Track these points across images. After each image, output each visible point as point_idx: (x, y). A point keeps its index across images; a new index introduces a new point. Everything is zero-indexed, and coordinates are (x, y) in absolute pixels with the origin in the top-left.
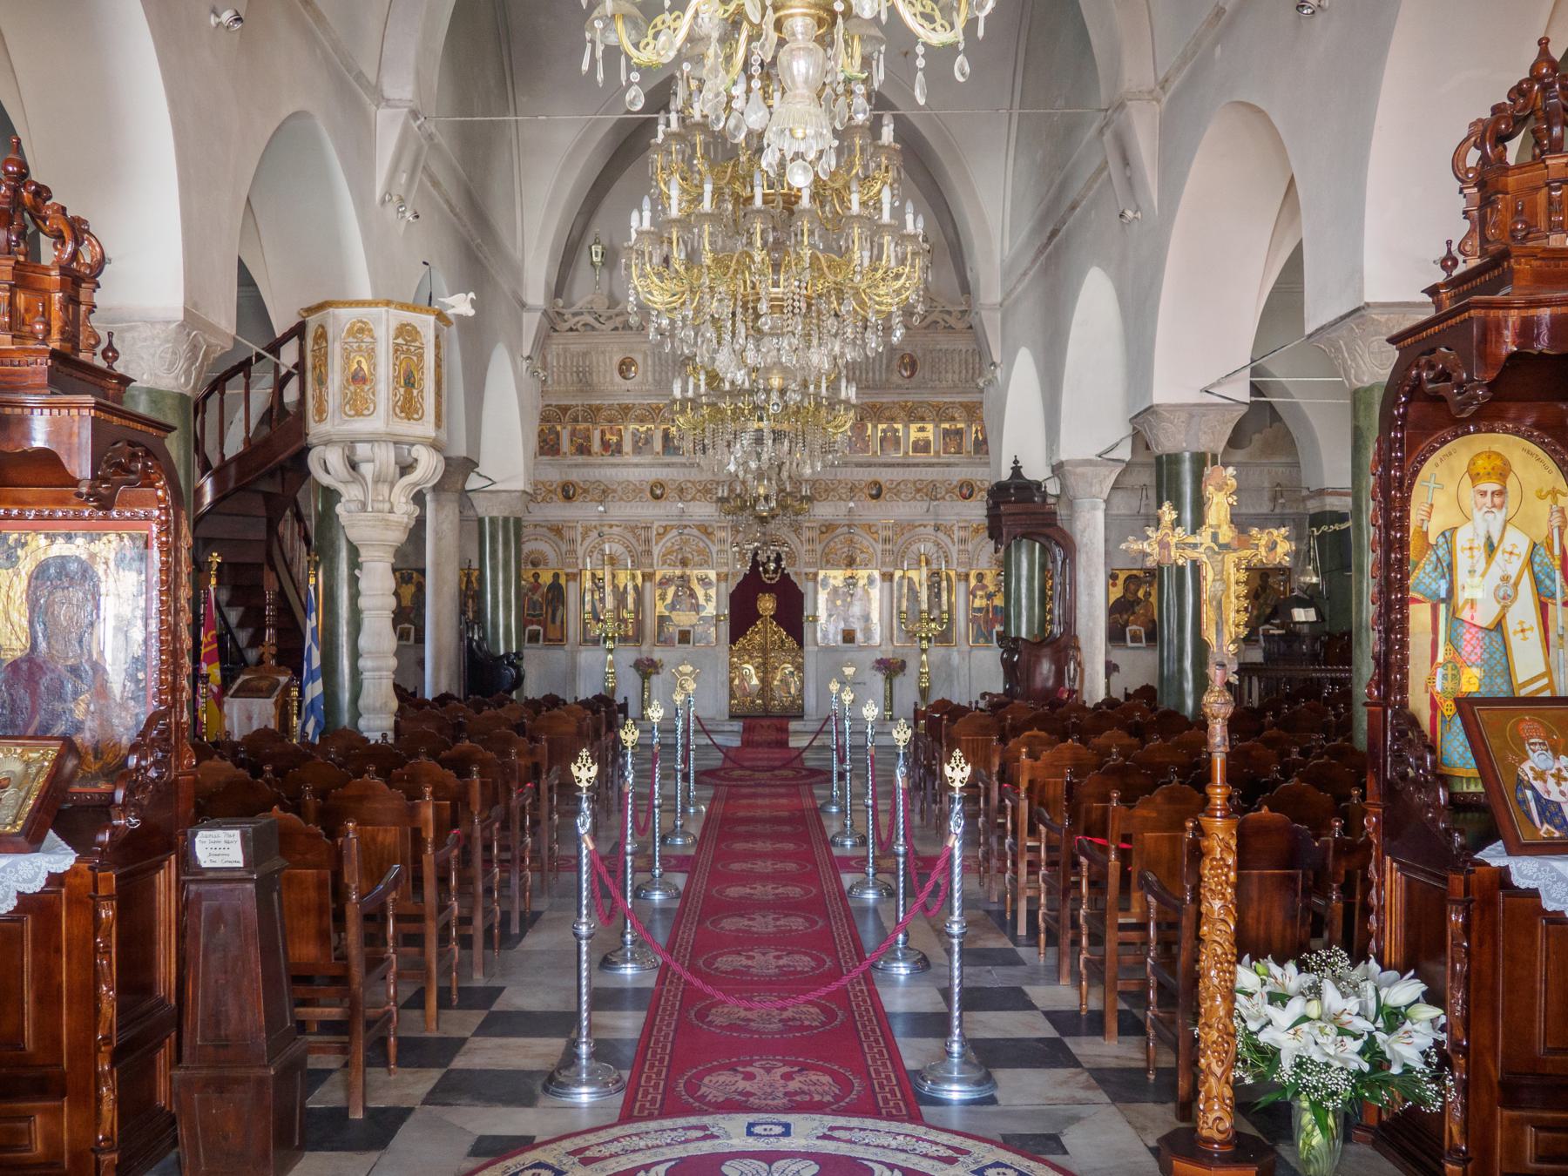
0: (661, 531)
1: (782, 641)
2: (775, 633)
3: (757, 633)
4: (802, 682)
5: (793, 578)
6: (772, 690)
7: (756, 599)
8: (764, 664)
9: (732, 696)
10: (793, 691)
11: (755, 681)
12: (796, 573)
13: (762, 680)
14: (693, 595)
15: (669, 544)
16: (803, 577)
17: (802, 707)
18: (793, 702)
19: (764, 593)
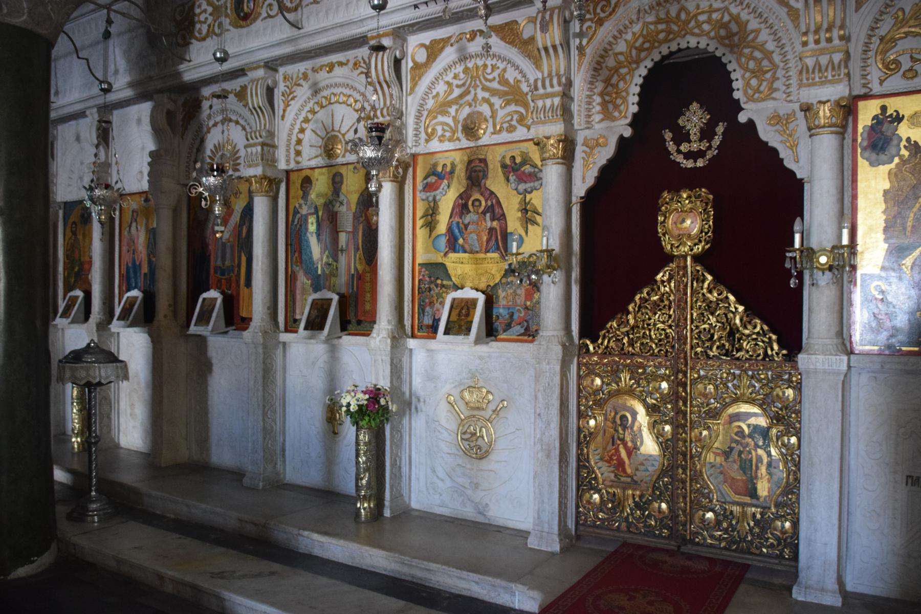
0: (422, 57)
1: (733, 332)
2: (711, 308)
3: (656, 307)
4: (793, 459)
5: (767, 134)
6: (696, 476)
7: (655, 210)
8: (675, 397)
9: (585, 483)
10: (763, 488)
11: (650, 446)
12: (776, 119)
13: (665, 445)
14: (495, 210)
15: (441, 88)
16: (801, 124)
17: (791, 542)
18: (764, 524)
19: (676, 190)
